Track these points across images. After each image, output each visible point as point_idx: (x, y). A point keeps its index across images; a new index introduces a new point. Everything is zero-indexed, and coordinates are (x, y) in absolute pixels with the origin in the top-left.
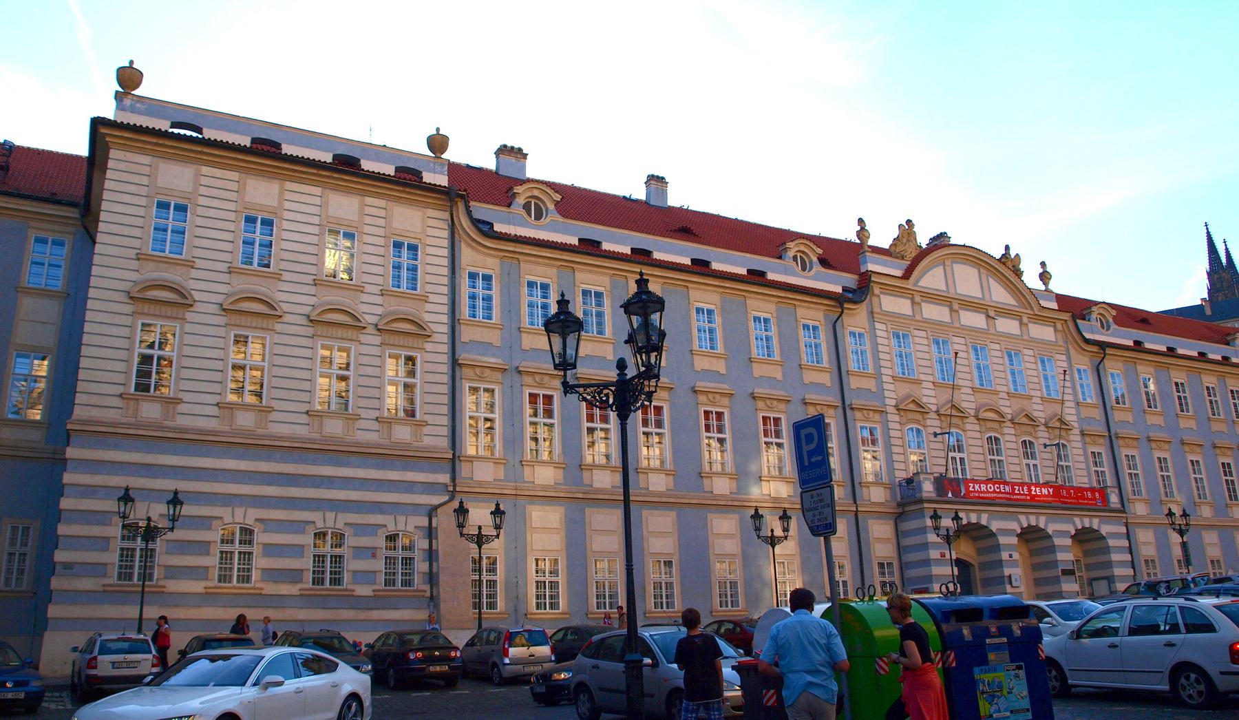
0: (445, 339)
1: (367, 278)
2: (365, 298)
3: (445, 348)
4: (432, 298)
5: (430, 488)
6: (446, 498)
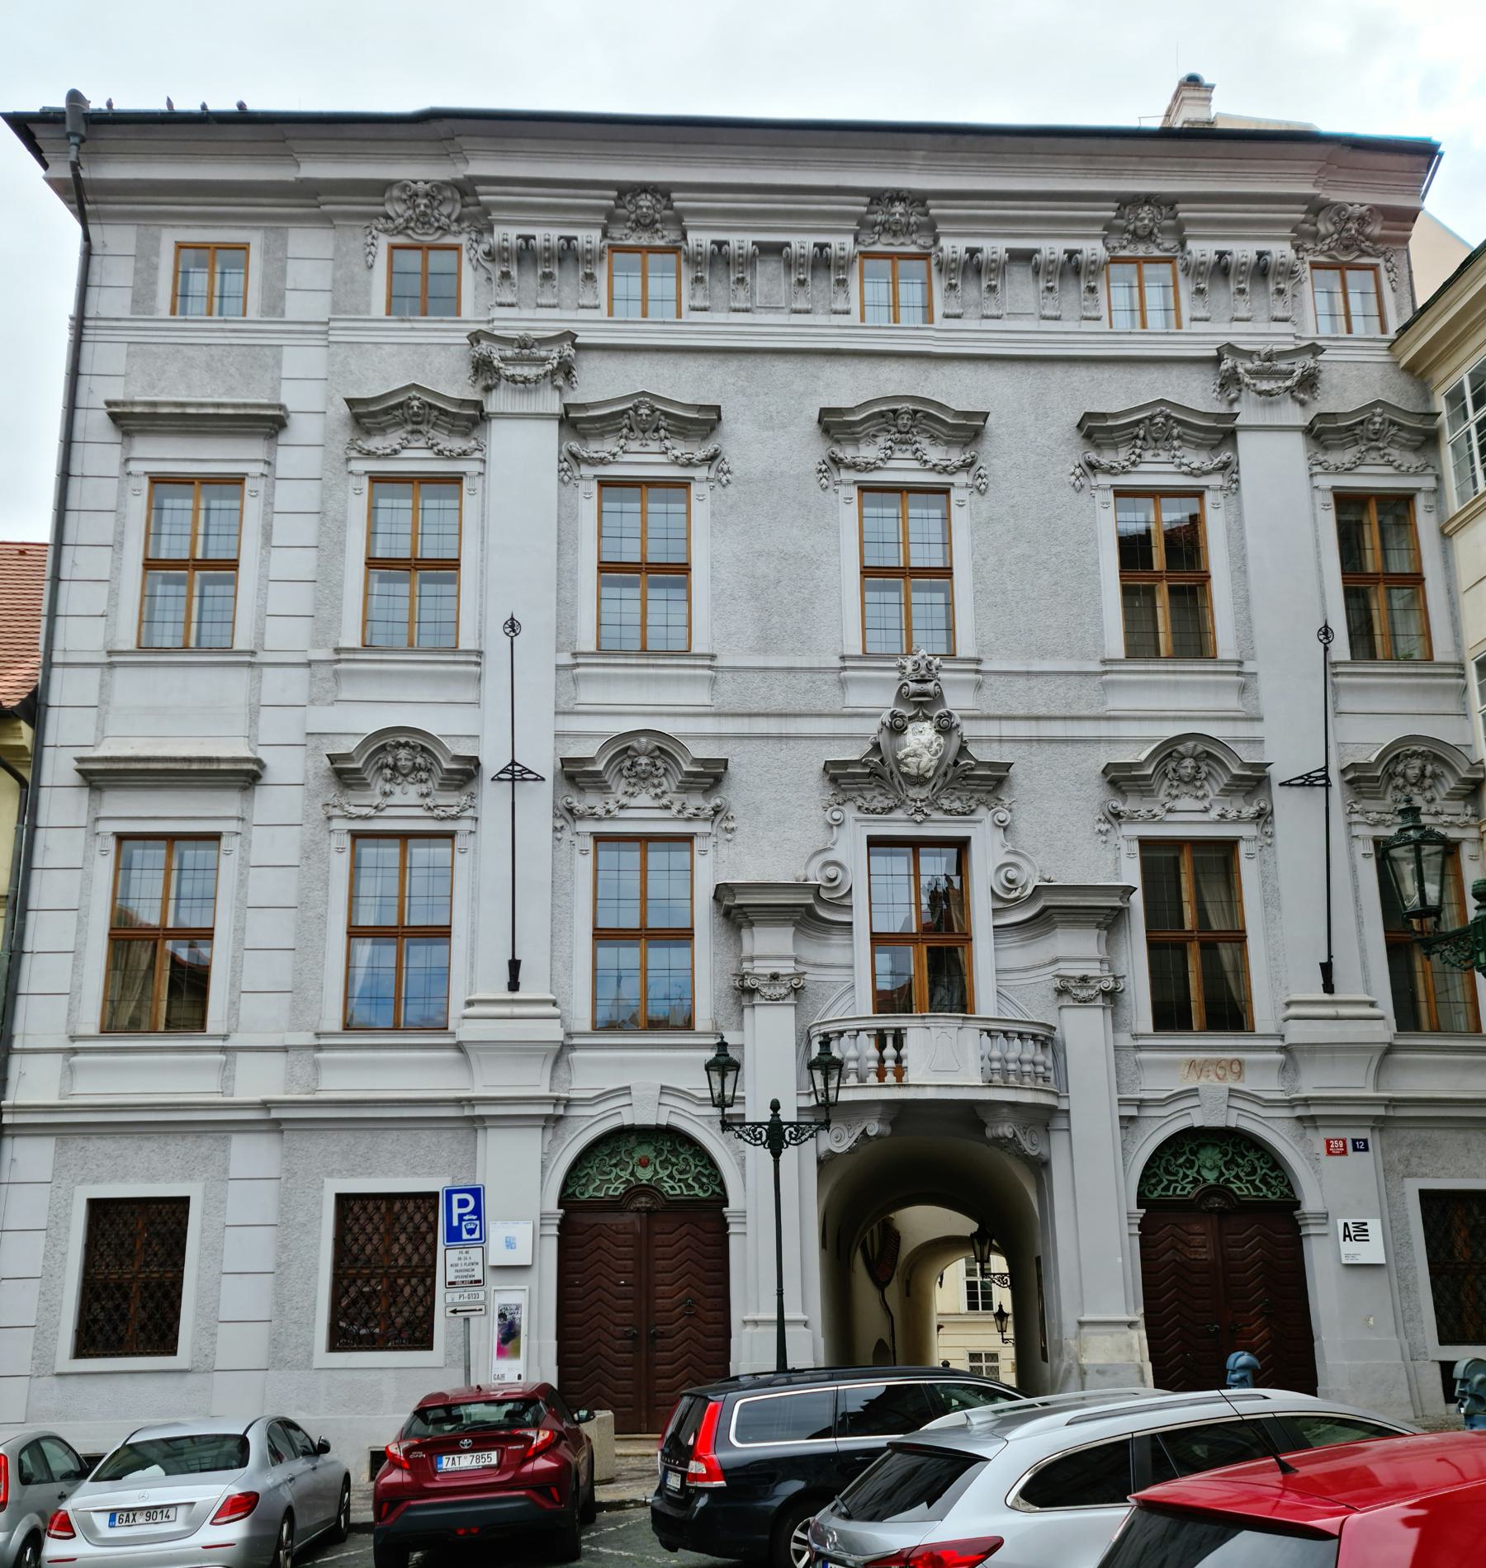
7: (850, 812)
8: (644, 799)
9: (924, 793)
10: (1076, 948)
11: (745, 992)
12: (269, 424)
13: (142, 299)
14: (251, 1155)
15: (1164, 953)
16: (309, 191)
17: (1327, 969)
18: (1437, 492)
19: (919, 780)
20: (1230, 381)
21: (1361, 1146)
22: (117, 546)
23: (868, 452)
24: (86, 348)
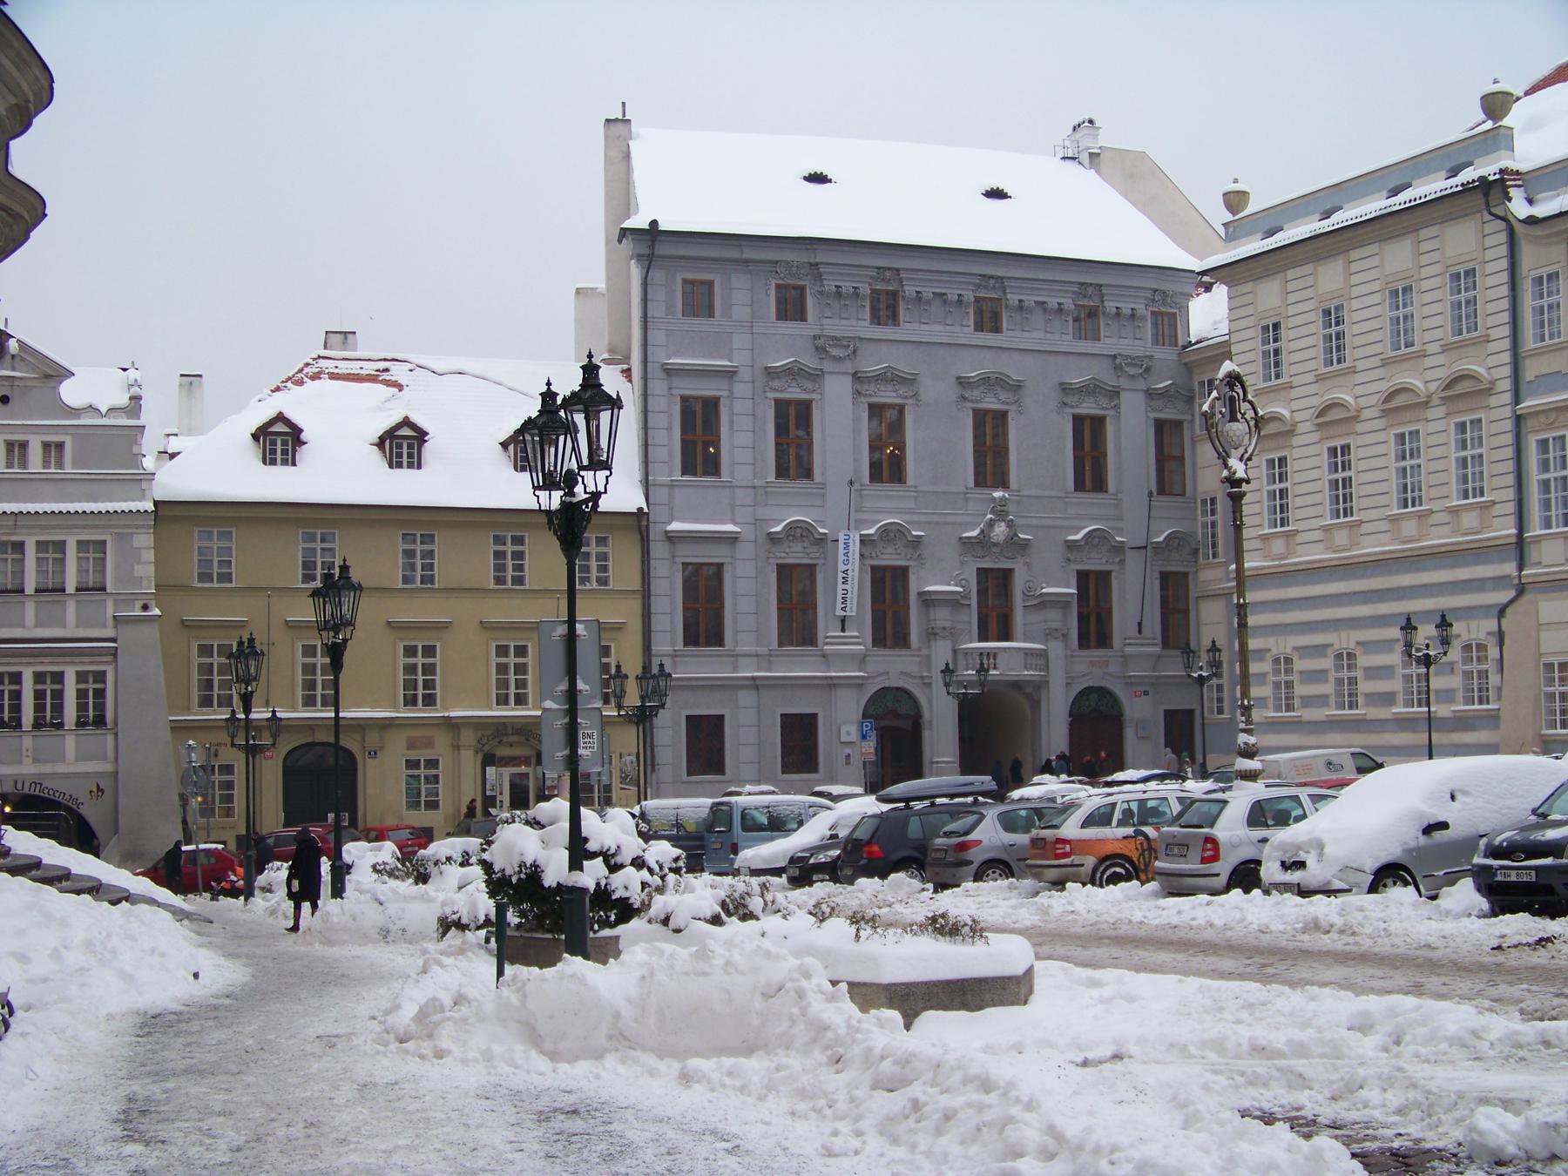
0: (1506, 385)
1: (1428, 336)
2: (1428, 362)
3: (1507, 398)
4: (1494, 334)
5: (1500, 582)
6: (1512, 593)
7: (968, 558)
8: (890, 550)
9: (995, 550)
10: (1053, 617)
11: (931, 634)
12: (730, 374)
13: (669, 309)
14: (746, 698)
15: (1083, 619)
16: (746, 262)
17: (1140, 624)
18: (1192, 422)
19: (995, 545)
20: (1117, 368)
21: (1146, 693)
22: (669, 429)
23: (976, 393)
24: (649, 333)
